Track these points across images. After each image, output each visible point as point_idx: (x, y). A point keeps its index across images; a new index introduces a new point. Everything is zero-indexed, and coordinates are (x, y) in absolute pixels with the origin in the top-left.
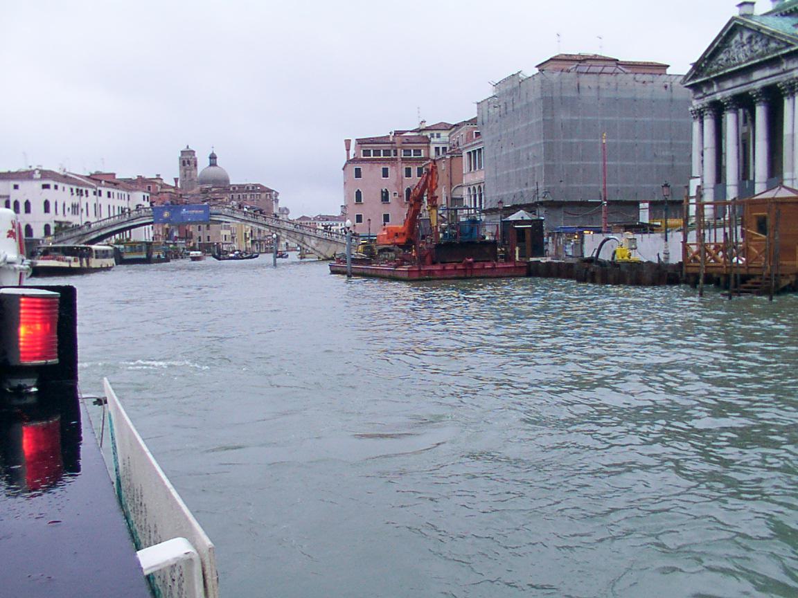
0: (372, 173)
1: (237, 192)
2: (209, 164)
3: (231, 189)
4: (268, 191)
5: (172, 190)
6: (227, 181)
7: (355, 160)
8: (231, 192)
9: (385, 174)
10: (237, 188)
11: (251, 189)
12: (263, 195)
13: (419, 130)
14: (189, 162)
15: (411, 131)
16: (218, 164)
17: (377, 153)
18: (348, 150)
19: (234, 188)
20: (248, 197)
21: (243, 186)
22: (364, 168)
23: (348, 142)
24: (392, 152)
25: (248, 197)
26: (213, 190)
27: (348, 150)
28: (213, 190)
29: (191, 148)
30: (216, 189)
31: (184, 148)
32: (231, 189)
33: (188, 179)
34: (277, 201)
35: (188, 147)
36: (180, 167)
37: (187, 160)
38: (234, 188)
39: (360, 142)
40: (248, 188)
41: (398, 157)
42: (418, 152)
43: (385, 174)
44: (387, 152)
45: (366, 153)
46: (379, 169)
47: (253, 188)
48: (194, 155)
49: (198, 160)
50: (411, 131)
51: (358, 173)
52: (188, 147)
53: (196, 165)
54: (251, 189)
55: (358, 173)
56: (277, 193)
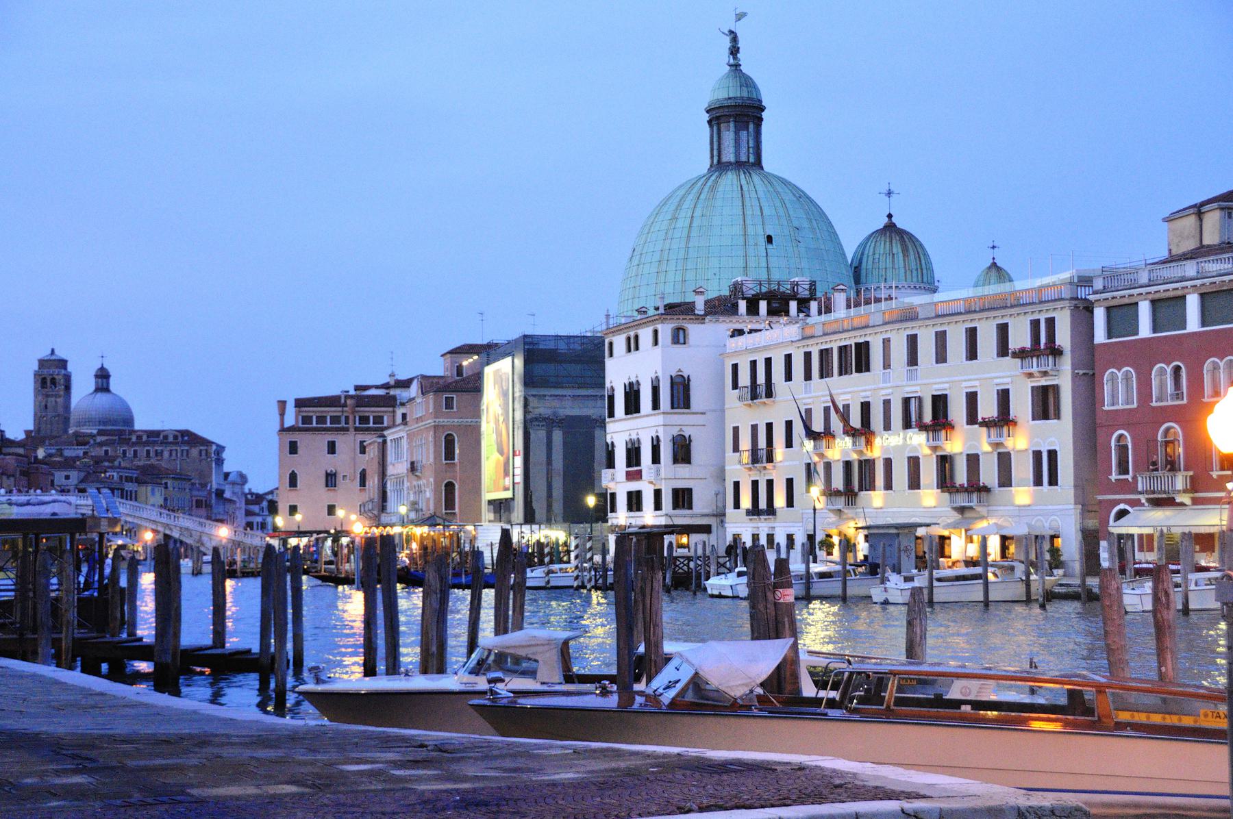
0: (313, 444)
1: (147, 443)
2: (93, 388)
3: (134, 439)
4: (202, 445)
5: (21, 451)
6: (129, 421)
7: (292, 429)
8: (134, 444)
9: (332, 448)
10: (145, 438)
11: (171, 439)
12: (194, 452)
13: (386, 386)
14: (53, 381)
15: (377, 387)
16: (111, 388)
17: (321, 419)
18: (282, 414)
19: (139, 437)
20: (166, 454)
21: (155, 434)
22: (301, 439)
23: (282, 404)
24: (343, 419)
25: (166, 454)
26: (99, 439)
27: (282, 414)
28: (99, 439)
29: (61, 354)
30: (104, 438)
31: (44, 353)
32: (134, 439)
33: (50, 414)
34: (220, 462)
35: (53, 351)
36: (35, 389)
37: (52, 378)
38: (139, 437)
39: (300, 403)
40: (166, 437)
41: (351, 425)
42: (379, 420)
43: (332, 448)
44: (335, 420)
45: (307, 420)
46: (322, 440)
47: (175, 437)
48: (65, 368)
49: (73, 378)
50: (377, 387)
51: (293, 448)
52: (53, 351)
53: (68, 388)
54: (171, 439)
55: (293, 448)
56: (221, 449)
